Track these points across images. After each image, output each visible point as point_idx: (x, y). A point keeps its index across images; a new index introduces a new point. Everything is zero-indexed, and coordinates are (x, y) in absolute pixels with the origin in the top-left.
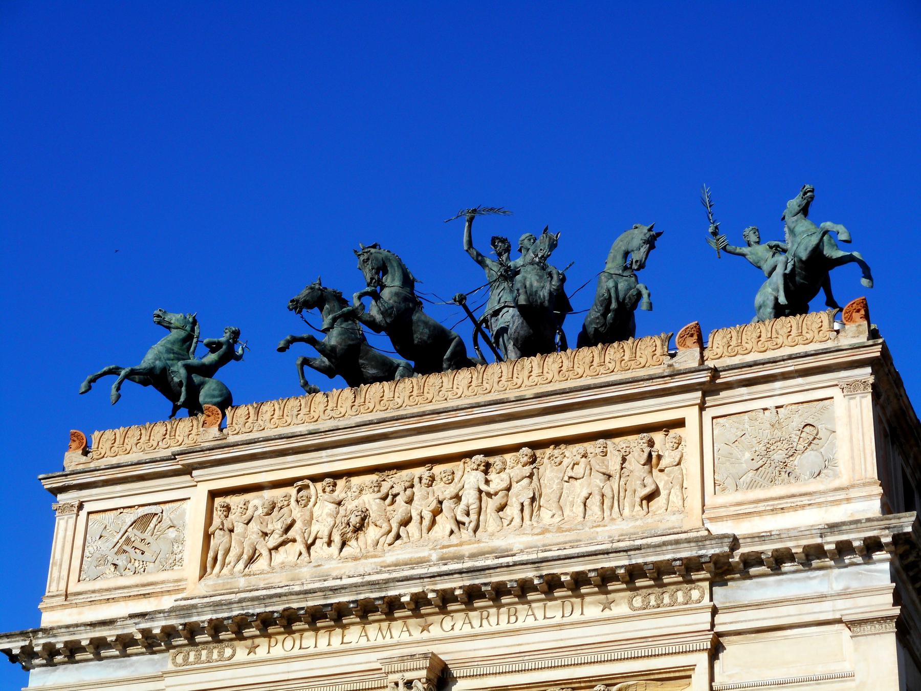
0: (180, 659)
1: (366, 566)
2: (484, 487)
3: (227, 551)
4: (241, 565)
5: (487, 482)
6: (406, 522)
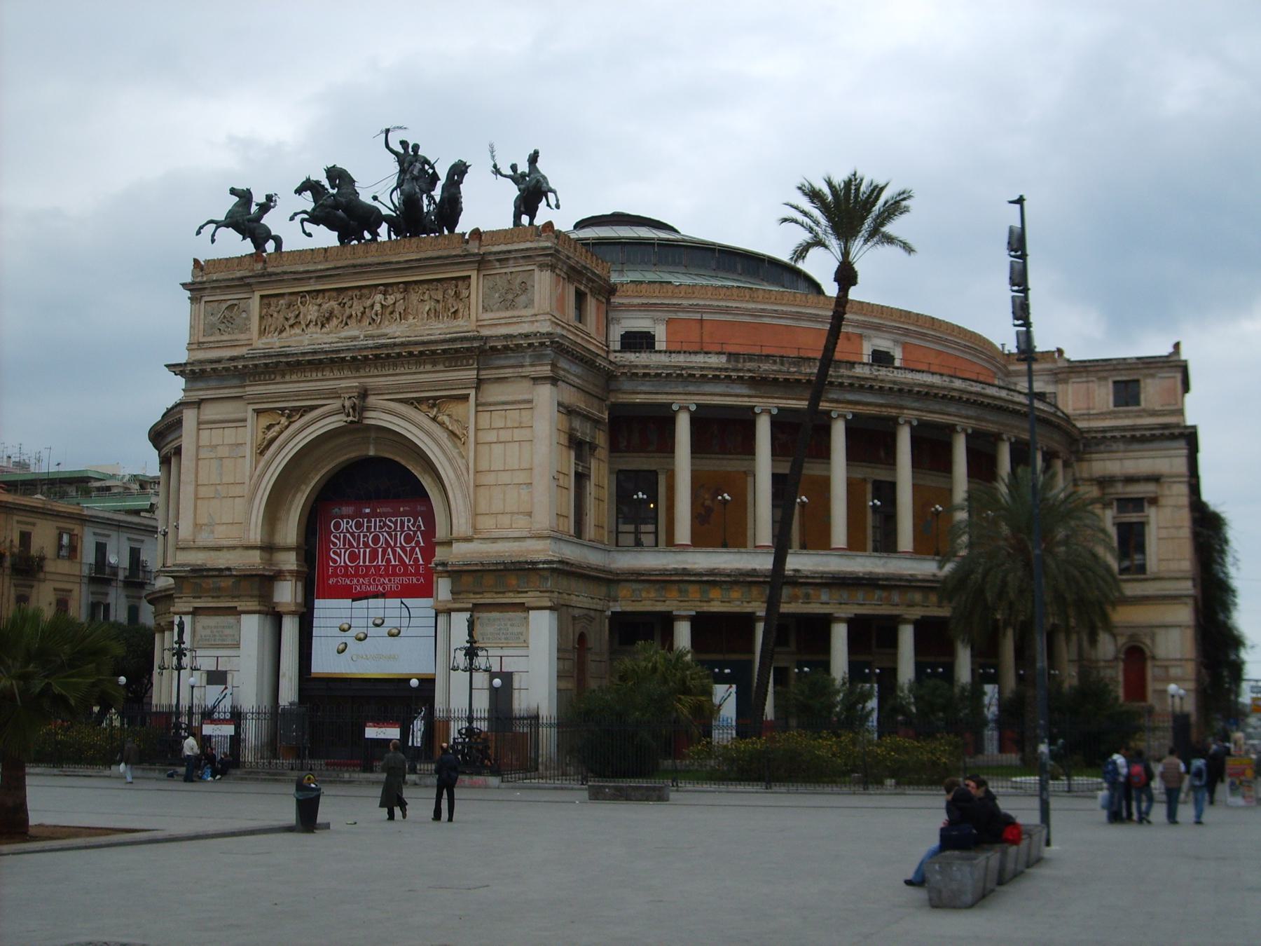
1: (332, 338)
2: (383, 303)
3: (270, 326)
4: (276, 333)
5: (386, 299)
6: (350, 317)
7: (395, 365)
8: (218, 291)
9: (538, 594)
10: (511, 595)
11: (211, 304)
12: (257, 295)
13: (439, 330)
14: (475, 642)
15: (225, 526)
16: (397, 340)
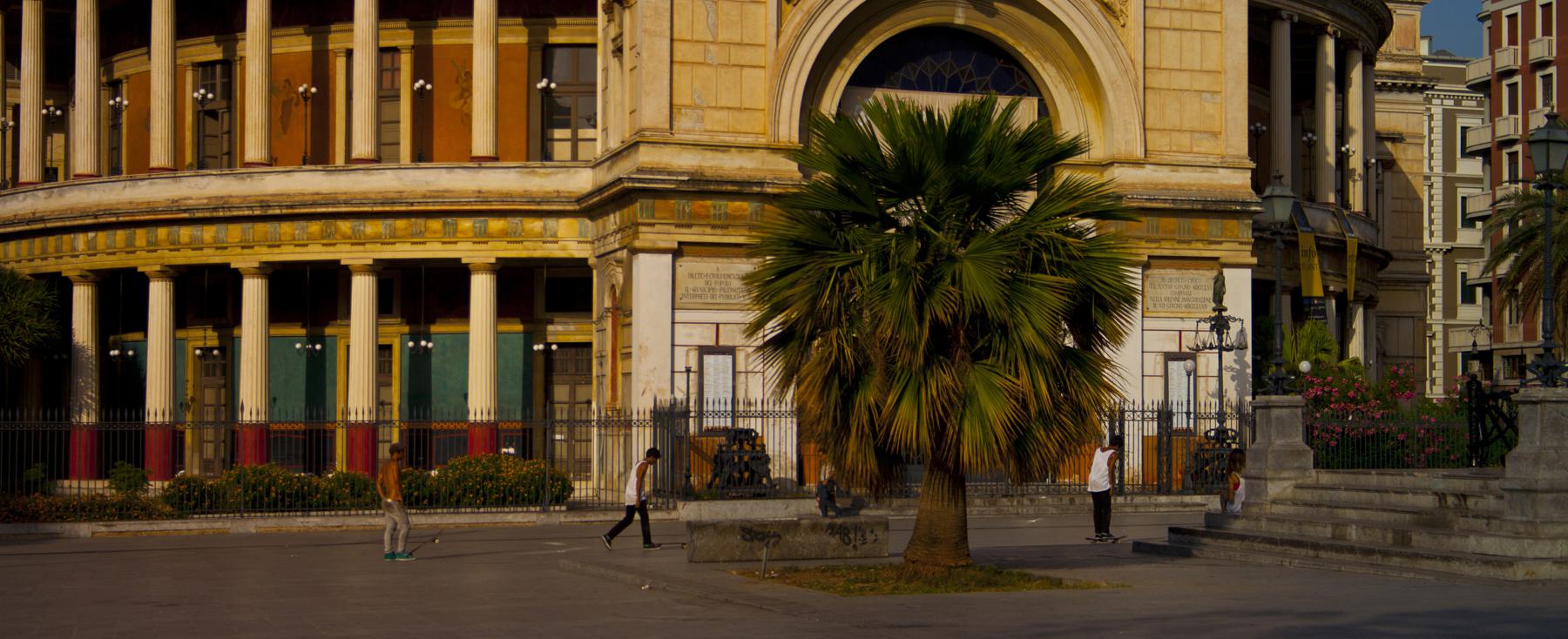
9: (1236, 246)
10: (1200, 245)
14: (1225, 310)
15: (725, 113)
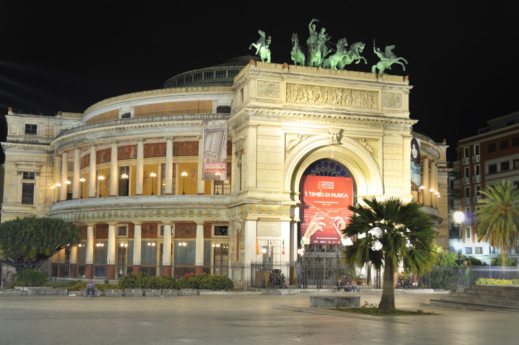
0: (285, 119)
2: (342, 96)
4: (294, 100)
5: (343, 95)
7: (350, 123)
8: (265, 77)
11: (260, 82)
12: (285, 82)
13: (366, 111)
16: (351, 112)
